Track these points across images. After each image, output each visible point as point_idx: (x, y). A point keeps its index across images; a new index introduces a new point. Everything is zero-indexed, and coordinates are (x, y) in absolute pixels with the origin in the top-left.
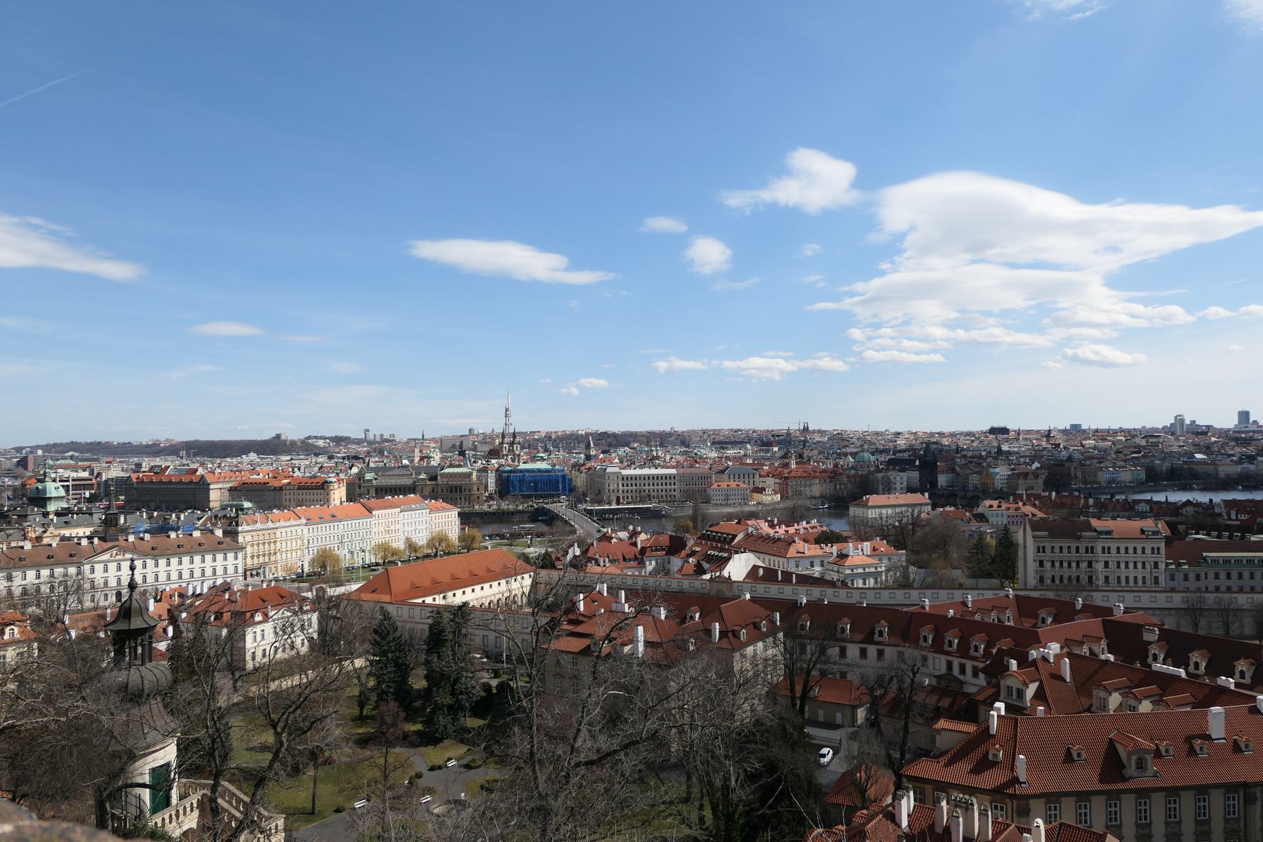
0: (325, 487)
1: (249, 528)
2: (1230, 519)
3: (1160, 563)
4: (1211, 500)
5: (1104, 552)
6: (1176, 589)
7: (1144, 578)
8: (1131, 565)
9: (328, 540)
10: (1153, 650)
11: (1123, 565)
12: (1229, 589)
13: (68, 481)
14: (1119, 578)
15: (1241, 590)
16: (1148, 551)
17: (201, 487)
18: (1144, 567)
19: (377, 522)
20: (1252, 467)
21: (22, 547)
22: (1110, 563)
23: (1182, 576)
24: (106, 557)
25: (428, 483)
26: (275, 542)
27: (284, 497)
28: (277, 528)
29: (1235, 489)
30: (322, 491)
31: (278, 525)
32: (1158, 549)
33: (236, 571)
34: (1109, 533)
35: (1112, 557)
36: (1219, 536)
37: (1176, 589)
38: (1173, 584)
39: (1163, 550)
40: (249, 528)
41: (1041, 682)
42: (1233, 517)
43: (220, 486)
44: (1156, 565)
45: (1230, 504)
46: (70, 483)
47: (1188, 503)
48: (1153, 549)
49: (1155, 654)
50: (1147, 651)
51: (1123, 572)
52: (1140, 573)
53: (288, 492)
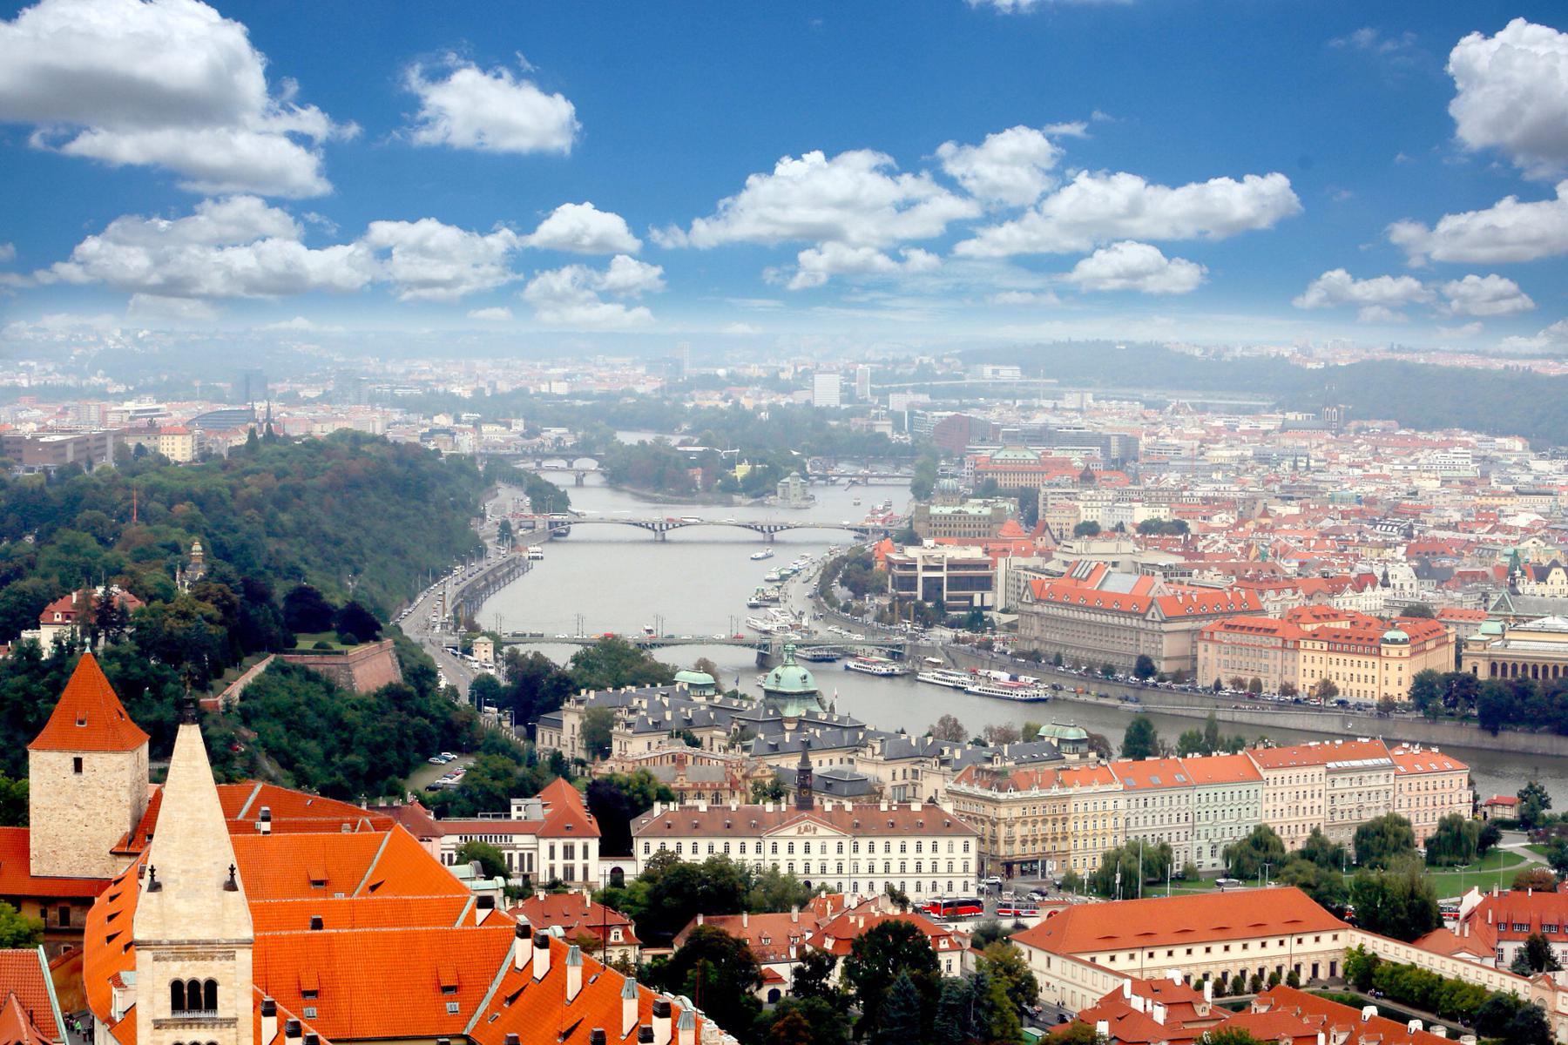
0: (1383, 653)
1: (1018, 795)
9: (1166, 821)
13: (940, 568)
17: (1150, 626)
19: (1271, 792)
21: (697, 808)
24: (792, 831)
26: (1065, 820)
27: (1302, 666)
28: (1068, 797)
29: (1397, 970)
30: (1377, 661)
33: (966, 867)
40: (1018, 795)
46: (943, 574)
53: (1309, 655)
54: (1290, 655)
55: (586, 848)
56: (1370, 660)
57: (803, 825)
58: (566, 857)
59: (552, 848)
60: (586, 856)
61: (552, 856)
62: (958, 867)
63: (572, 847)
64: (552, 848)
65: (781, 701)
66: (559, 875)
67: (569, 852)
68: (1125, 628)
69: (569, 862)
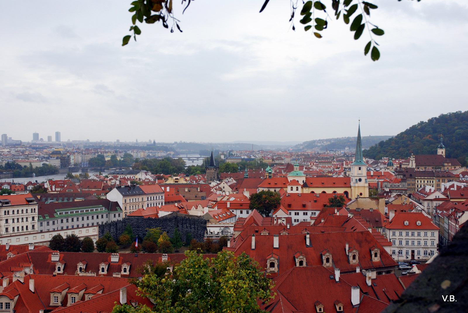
2: (52, 191)
3: (35, 217)
4: (36, 181)
5: (5, 214)
6: (43, 231)
7: (27, 227)
8: (20, 220)
10: (59, 265)
11: (16, 221)
12: (73, 228)
14: (13, 228)
15: (83, 227)
16: (29, 211)
18: (27, 221)
20: (47, 163)
22: (9, 220)
23: (46, 223)
32: (35, 209)
34: (7, 203)
35: (10, 217)
36: (57, 200)
37: (43, 231)
38: (42, 228)
39: (37, 211)
41: (19, 295)
42: (54, 189)
44: (33, 218)
45: (51, 182)
47: (30, 183)
48: (32, 210)
49: (59, 267)
50: (55, 266)
51: (16, 225)
52: (25, 224)
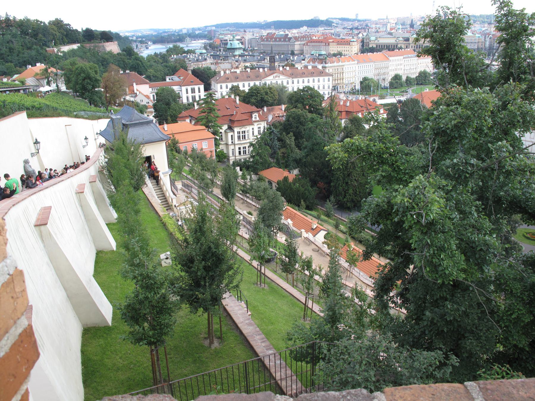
21: (236, 72)
25: (405, 42)
28: (343, 66)
31: (344, 64)
43: (299, 43)
54: (327, 47)
55: (199, 89)
56: (347, 46)
57: (275, 75)
58: (192, 93)
59: (187, 90)
60: (199, 92)
61: (187, 93)
62: (326, 87)
63: (194, 89)
64: (187, 90)
65: (233, 51)
66: (191, 101)
67: (193, 91)
68: (285, 45)
69: (193, 94)
